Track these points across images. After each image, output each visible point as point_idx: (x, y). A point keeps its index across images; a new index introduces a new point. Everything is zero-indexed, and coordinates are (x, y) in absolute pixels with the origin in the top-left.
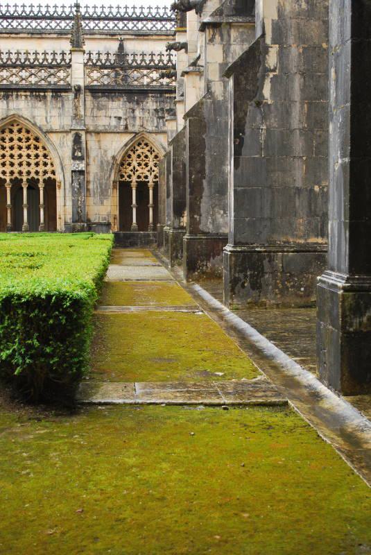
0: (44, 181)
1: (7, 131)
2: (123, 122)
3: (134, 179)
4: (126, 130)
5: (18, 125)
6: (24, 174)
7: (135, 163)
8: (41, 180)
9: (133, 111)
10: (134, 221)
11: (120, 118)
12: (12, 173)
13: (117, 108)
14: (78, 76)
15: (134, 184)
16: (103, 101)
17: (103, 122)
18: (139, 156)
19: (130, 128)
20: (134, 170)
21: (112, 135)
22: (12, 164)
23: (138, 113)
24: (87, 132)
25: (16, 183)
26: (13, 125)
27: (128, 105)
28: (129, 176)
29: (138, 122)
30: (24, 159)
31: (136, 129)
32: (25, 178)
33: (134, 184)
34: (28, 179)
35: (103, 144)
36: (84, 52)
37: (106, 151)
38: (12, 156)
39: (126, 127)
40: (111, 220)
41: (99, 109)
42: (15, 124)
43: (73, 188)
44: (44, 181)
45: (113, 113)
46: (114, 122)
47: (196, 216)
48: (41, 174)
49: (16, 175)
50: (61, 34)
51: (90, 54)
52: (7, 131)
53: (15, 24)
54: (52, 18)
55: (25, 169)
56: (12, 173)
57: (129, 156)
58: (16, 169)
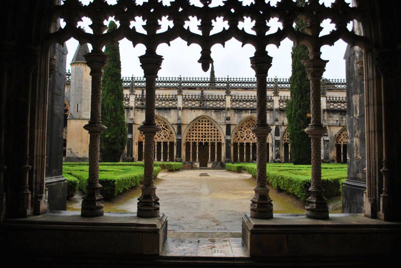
2: (338, 122)
3: (342, 143)
4: (340, 125)
7: (342, 137)
9: (342, 118)
10: (342, 159)
11: (337, 121)
13: (336, 117)
14: (228, 104)
15: (342, 145)
16: (331, 114)
17: (331, 122)
18: (344, 135)
19: (341, 125)
20: (342, 140)
21: (335, 127)
23: (344, 119)
24: (329, 126)
27: (341, 116)
28: (340, 142)
29: (344, 122)
31: (344, 125)
33: (342, 145)
35: (331, 130)
37: (332, 133)
39: (340, 124)
40: (335, 159)
41: (330, 117)
43: (325, 147)
45: (335, 119)
46: (335, 122)
47: (360, 158)
50: (223, 88)
51: (281, 97)
53: (283, 85)
54: (250, 83)
57: (340, 135)
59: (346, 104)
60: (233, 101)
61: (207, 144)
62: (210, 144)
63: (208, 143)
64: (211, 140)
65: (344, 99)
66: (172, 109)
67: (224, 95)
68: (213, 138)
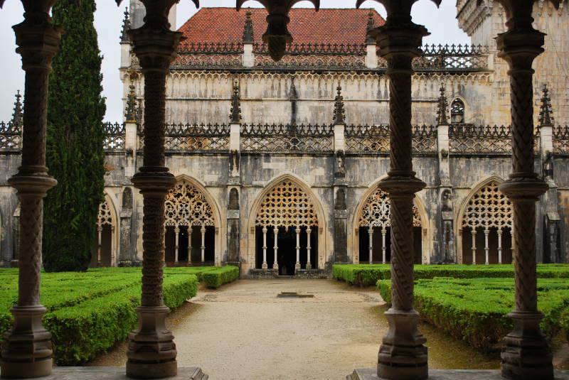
0: (300, 227)
1: (486, 189)
5: (495, 185)
6: (487, 223)
8: (500, 228)
12: (477, 222)
22: (477, 216)
25: (493, 231)
26: (490, 185)
30: (486, 212)
32: (500, 227)
34: (489, 229)
36: (552, 126)
38: (503, 209)
42: (493, 185)
44: (502, 229)
48: (500, 223)
49: (493, 224)
52: (486, 189)
55: (499, 219)
56: (477, 222)
58: (493, 219)
59: (508, 141)
60: (348, 136)
61: (292, 229)
62: (298, 230)
63: (295, 227)
64: (301, 222)
65: (506, 131)
66: (174, 154)
67: (120, 123)
68: (303, 219)
